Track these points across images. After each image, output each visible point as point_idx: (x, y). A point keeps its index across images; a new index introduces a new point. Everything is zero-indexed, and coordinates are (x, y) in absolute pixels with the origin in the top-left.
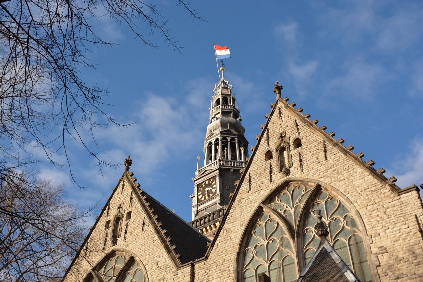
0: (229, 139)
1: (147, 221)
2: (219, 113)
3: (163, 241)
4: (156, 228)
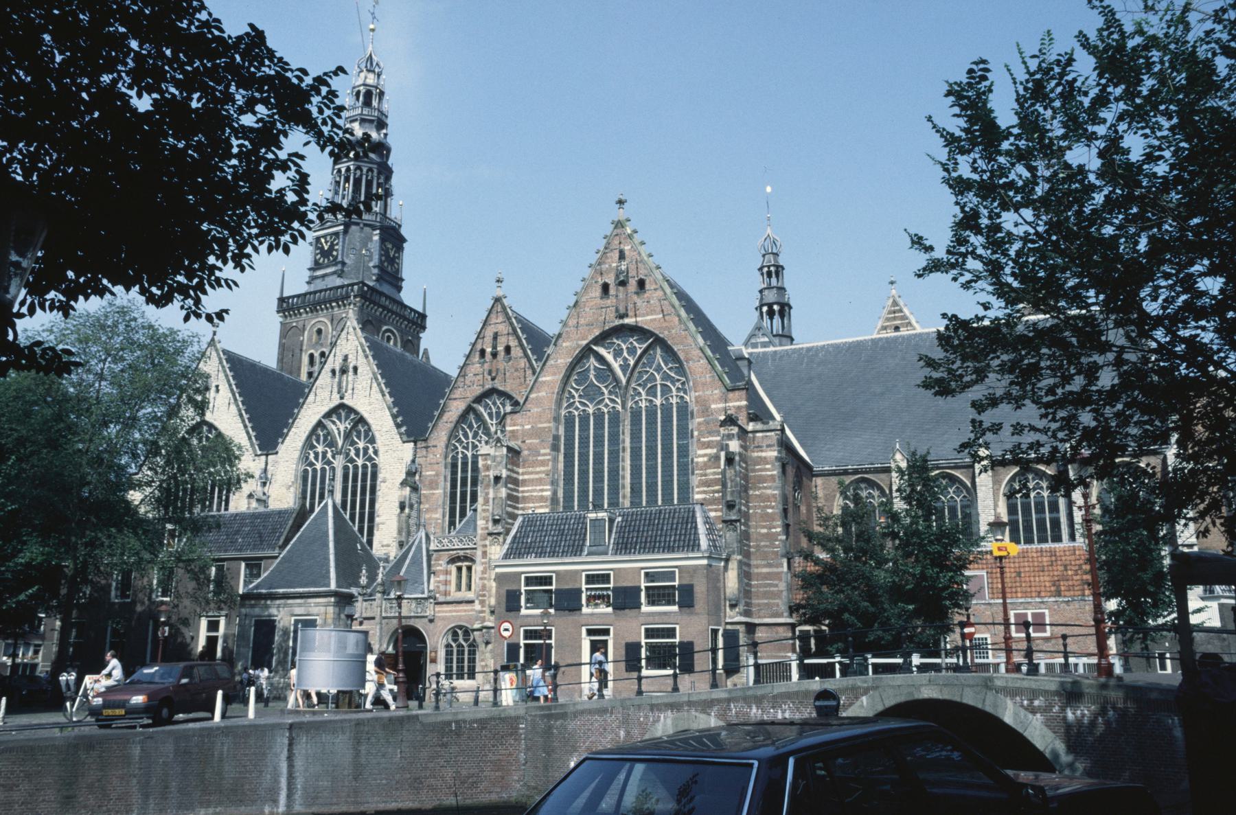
0: (365, 170)
1: (232, 401)
2: (356, 120)
3: (245, 427)
4: (239, 410)
